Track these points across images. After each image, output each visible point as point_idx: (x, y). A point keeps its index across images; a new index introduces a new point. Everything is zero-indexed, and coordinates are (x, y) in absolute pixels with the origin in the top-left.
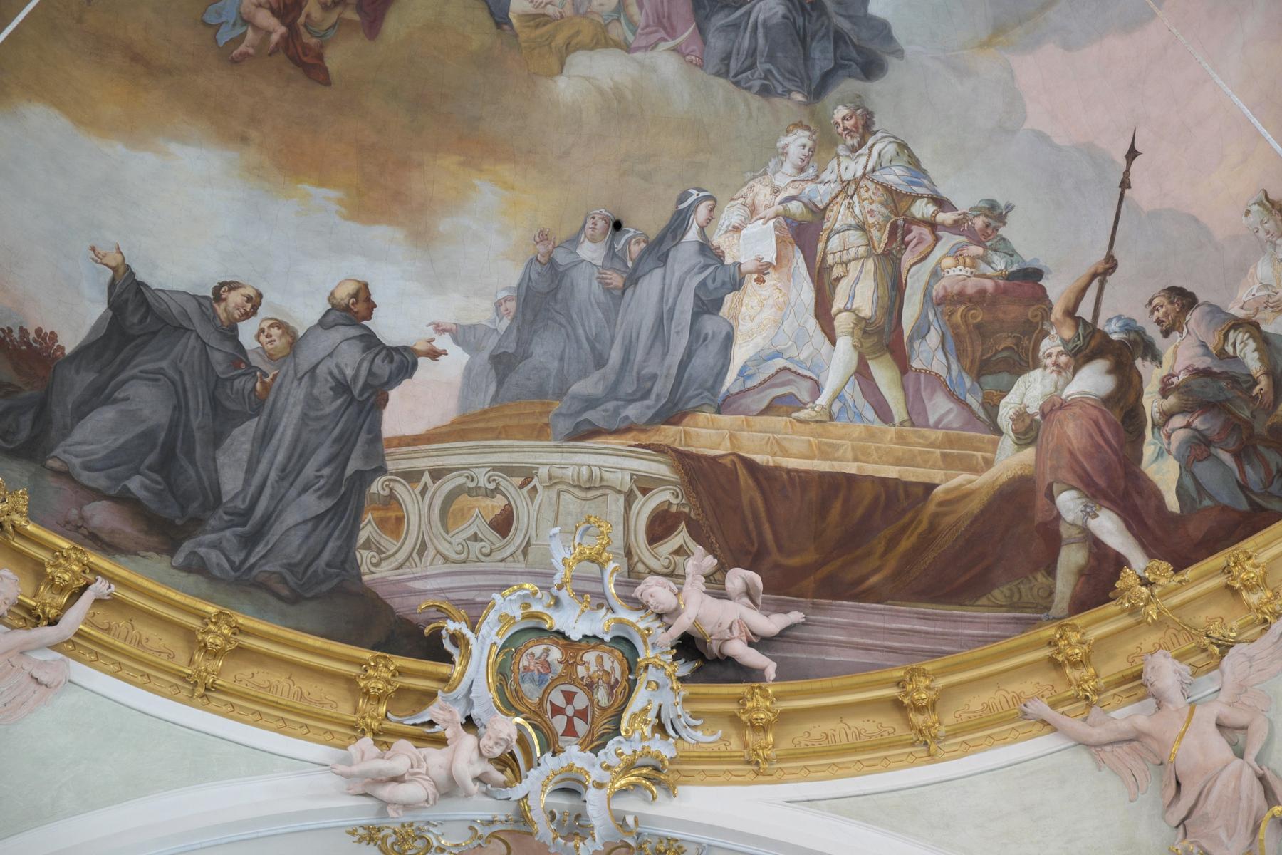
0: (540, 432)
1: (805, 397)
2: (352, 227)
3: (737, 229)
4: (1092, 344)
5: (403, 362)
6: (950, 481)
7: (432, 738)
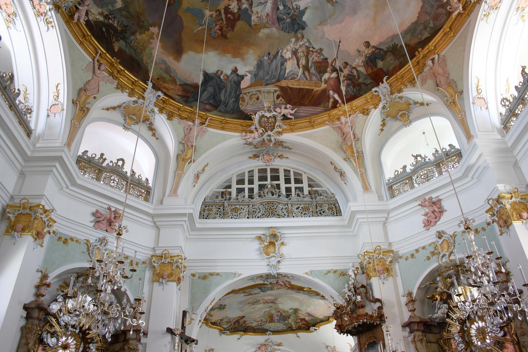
0: (261, 85)
2: (233, 59)
5: (242, 77)
6: (316, 89)
7: (252, 132)
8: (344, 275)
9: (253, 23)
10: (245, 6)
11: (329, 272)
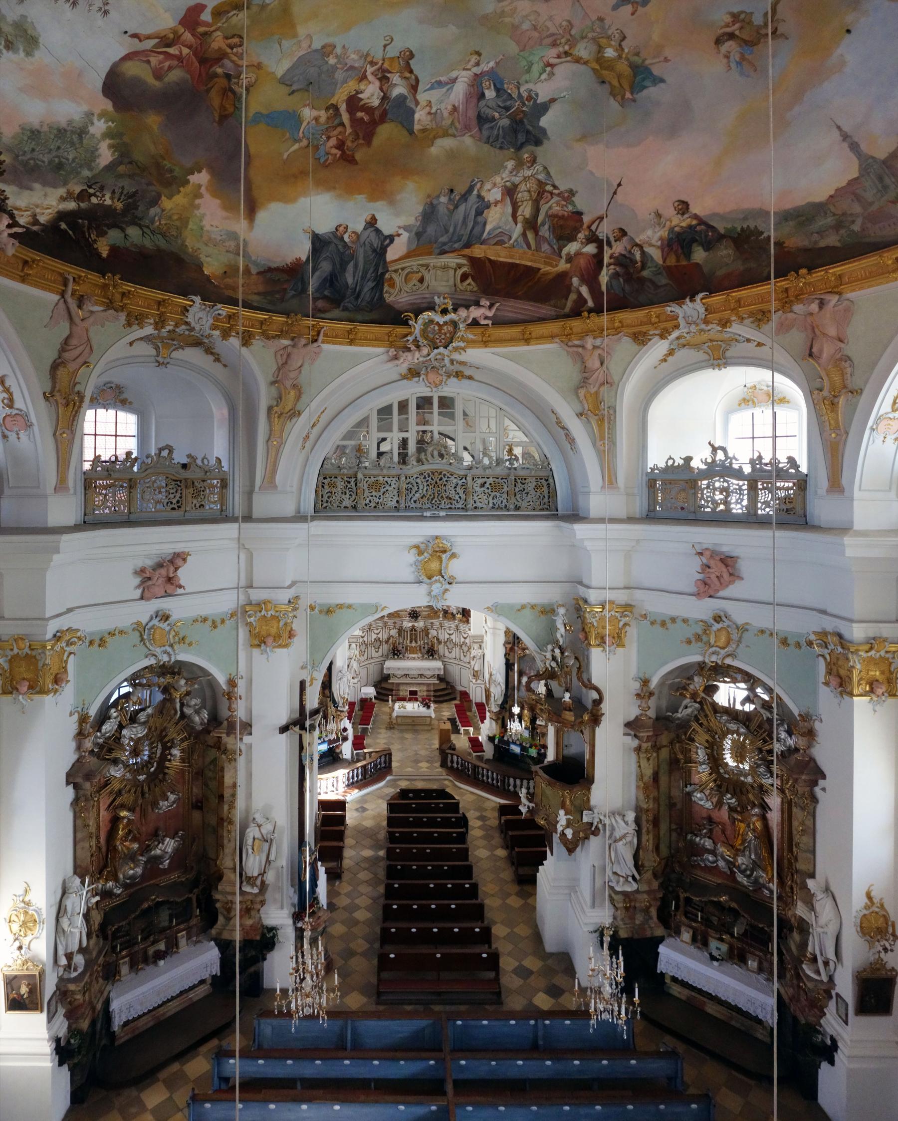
0: (430, 254)
1: (506, 240)
3: (489, 190)
4: (593, 238)
6: (545, 269)
9: (417, 127)
10: (399, 89)
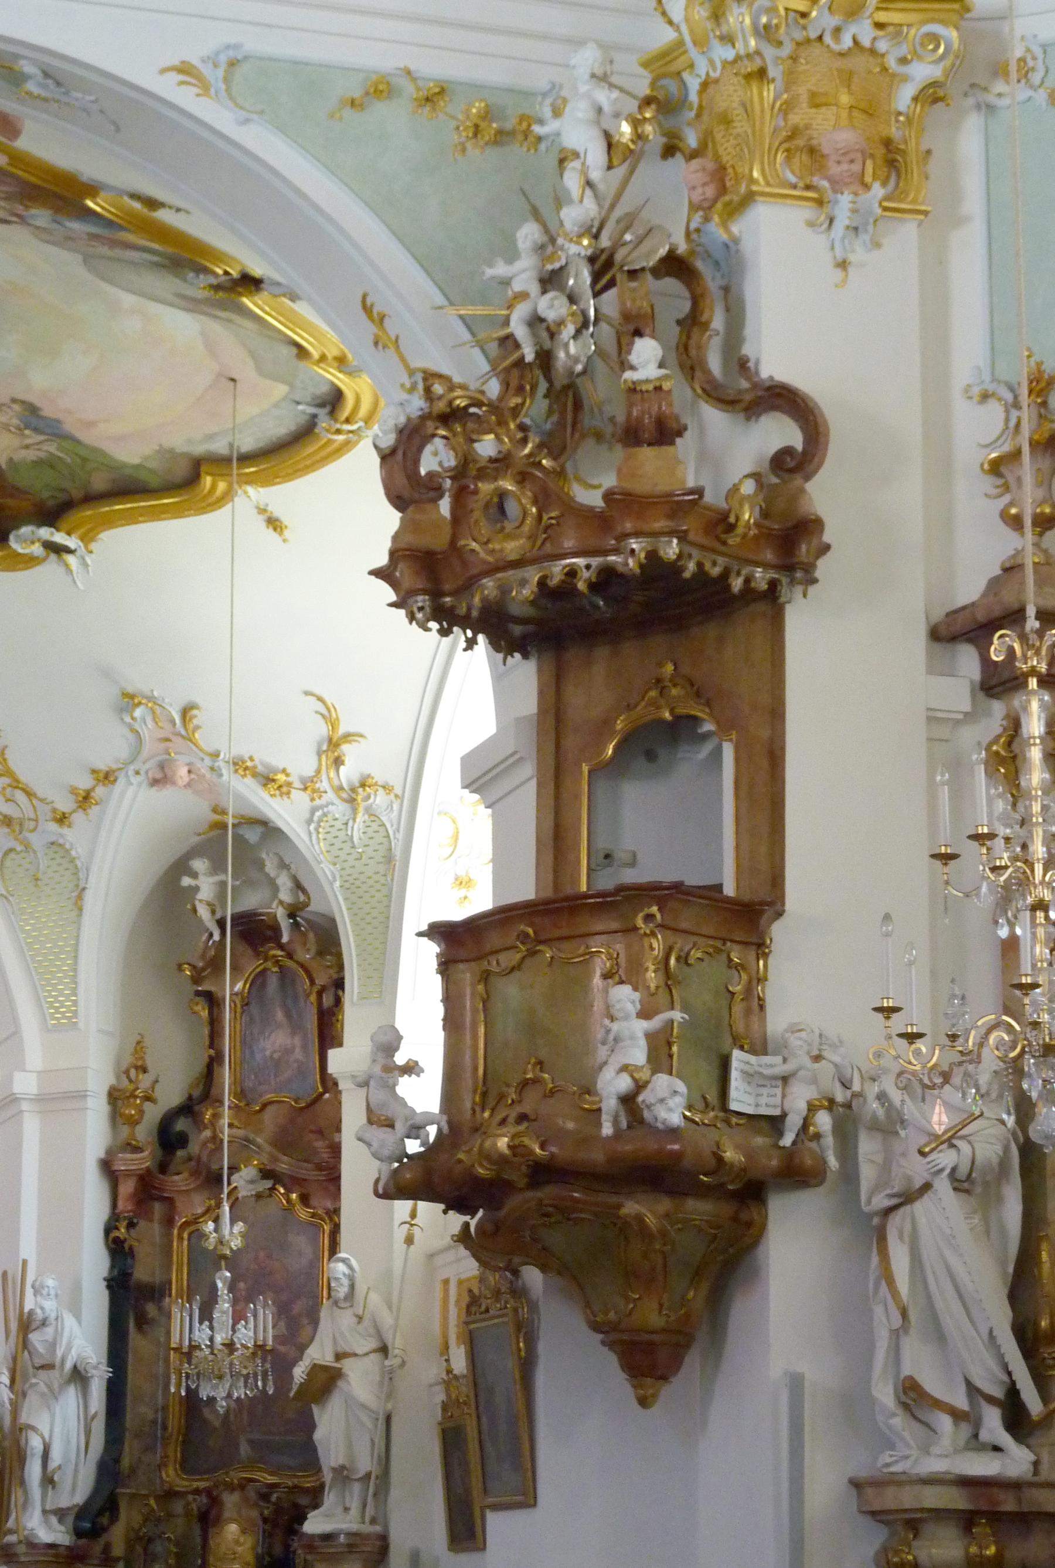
8: (502, 137)
11: (380, 89)
